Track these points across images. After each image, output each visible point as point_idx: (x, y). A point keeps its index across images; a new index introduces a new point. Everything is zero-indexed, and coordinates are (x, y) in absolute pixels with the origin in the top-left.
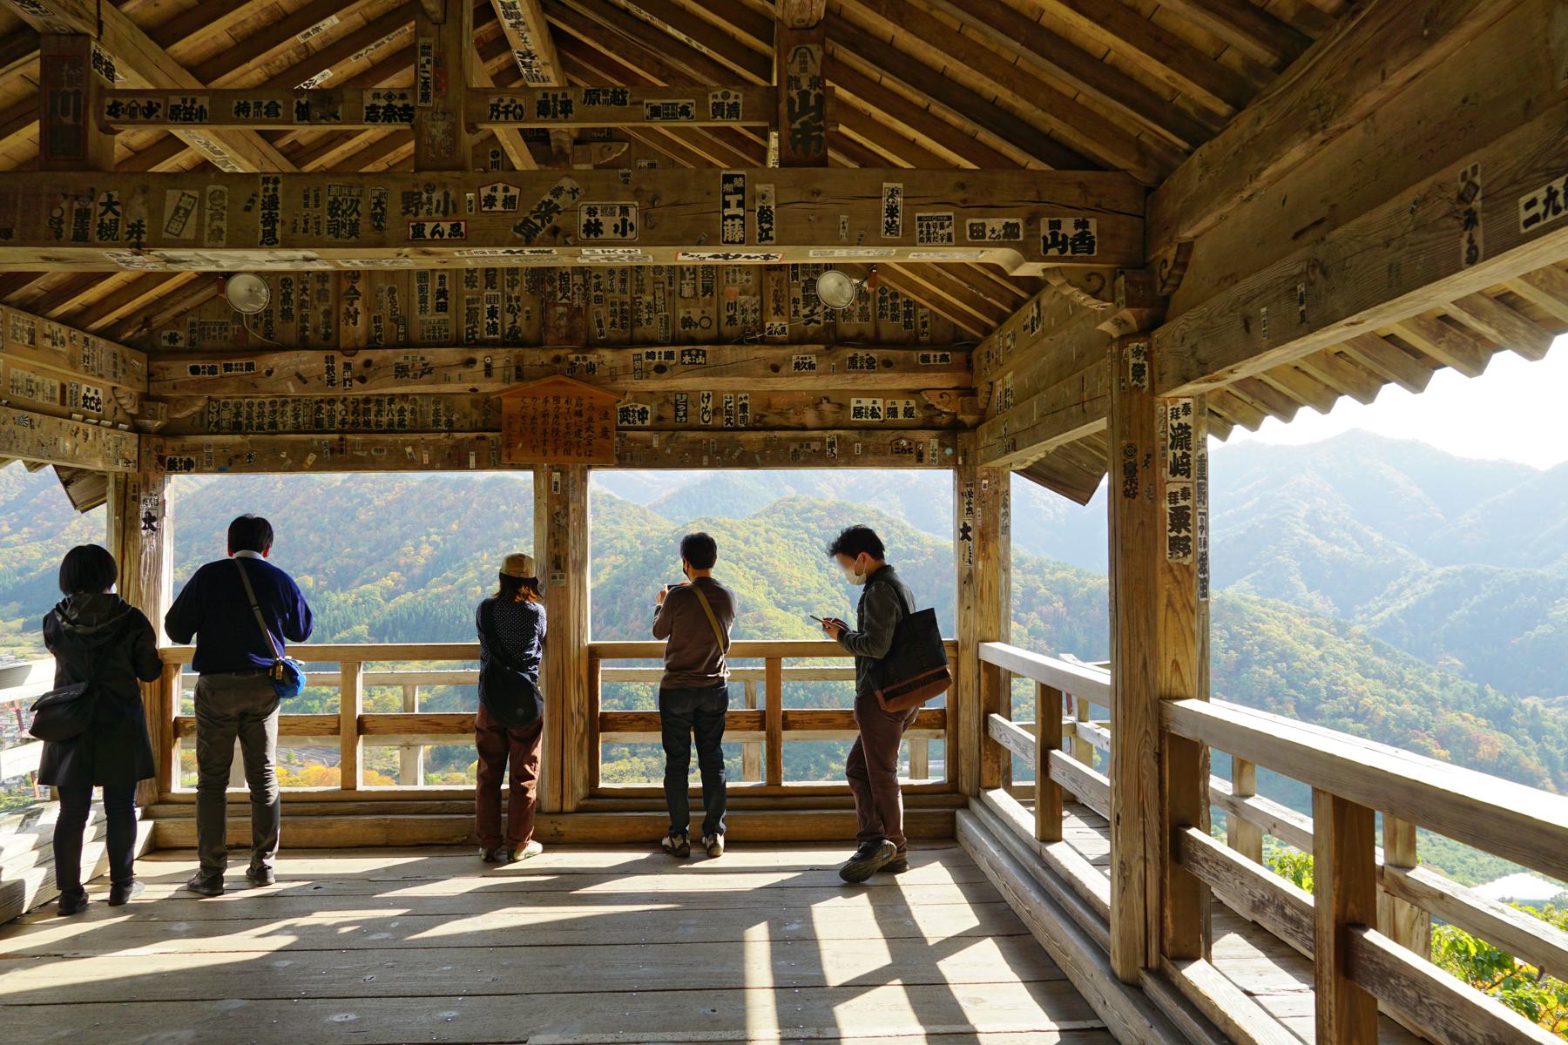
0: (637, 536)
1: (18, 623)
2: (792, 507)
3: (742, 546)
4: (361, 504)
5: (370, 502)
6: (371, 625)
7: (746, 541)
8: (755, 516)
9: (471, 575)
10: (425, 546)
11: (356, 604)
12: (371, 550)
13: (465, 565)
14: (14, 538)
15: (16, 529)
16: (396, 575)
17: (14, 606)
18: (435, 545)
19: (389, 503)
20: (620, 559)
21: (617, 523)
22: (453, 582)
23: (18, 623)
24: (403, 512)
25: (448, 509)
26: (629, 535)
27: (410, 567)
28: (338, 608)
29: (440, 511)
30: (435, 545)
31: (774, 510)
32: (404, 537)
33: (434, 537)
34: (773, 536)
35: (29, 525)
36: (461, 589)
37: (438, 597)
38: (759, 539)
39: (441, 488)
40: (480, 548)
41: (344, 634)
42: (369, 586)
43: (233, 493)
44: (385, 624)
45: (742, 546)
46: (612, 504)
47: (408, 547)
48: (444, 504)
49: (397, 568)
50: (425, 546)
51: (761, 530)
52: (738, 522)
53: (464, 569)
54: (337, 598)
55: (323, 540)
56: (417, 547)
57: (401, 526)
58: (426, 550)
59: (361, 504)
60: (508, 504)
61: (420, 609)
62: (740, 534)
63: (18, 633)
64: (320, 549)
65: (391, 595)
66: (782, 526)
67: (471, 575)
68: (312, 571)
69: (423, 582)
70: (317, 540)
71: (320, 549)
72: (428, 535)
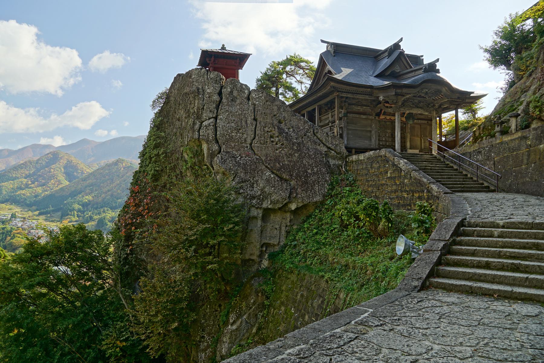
1: (37, 213)
14: (33, 185)
15: (33, 183)
17: (34, 208)
23: (37, 213)
35: (37, 181)
63: (37, 216)
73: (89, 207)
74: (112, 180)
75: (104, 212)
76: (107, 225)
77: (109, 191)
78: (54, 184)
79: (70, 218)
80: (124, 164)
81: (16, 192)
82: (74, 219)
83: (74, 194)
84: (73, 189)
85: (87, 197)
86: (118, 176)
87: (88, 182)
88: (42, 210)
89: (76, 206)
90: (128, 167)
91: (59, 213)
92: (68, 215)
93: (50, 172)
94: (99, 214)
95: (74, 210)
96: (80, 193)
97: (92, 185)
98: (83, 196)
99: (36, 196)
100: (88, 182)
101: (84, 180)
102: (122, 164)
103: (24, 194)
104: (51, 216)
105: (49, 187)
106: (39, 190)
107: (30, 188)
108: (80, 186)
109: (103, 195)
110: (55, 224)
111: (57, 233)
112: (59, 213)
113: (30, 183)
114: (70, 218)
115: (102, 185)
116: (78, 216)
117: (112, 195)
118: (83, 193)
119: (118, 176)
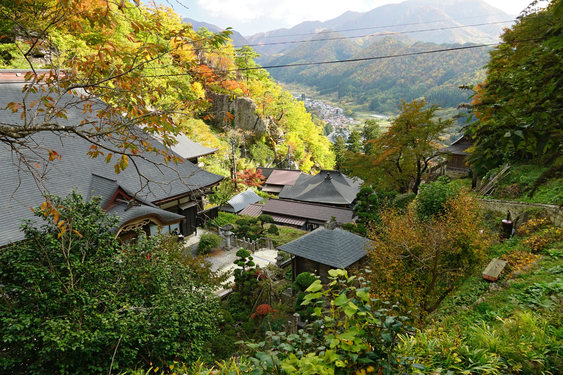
1: (319, 92)
11: (418, 89)
12: (422, 71)
16: (431, 80)
17: (315, 87)
18: (444, 69)
22: (453, 83)
23: (319, 92)
24: (433, 57)
25: (449, 55)
27: (436, 77)
29: (447, 56)
30: (444, 69)
37: (448, 88)
42: (423, 84)
43: (375, 51)
44: (430, 97)
49: (432, 77)
50: (441, 69)
55: (406, 67)
56: (438, 70)
57: (433, 62)
61: (442, 92)
64: (405, 70)
68: (403, 78)
69: (440, 83)
71: (405, 70)
73: (361, 87)
75: (375, 93)
77: (377, 71)
79: (346, 98)
80: (391, 42)
81: (299, 72)
84: (345, 69)
85: (359, 78)
89: (350, 87)
91: (337, 93)
92: (345, 95)
96: (352, 73)
98: (355, 77)
99: (315, 76)
103: (305, 74)
104: (330, 96)
111: (377, 133)
112: (337, 93)
115: (371, 65)
117: (381, 76)
118: (355, 74)
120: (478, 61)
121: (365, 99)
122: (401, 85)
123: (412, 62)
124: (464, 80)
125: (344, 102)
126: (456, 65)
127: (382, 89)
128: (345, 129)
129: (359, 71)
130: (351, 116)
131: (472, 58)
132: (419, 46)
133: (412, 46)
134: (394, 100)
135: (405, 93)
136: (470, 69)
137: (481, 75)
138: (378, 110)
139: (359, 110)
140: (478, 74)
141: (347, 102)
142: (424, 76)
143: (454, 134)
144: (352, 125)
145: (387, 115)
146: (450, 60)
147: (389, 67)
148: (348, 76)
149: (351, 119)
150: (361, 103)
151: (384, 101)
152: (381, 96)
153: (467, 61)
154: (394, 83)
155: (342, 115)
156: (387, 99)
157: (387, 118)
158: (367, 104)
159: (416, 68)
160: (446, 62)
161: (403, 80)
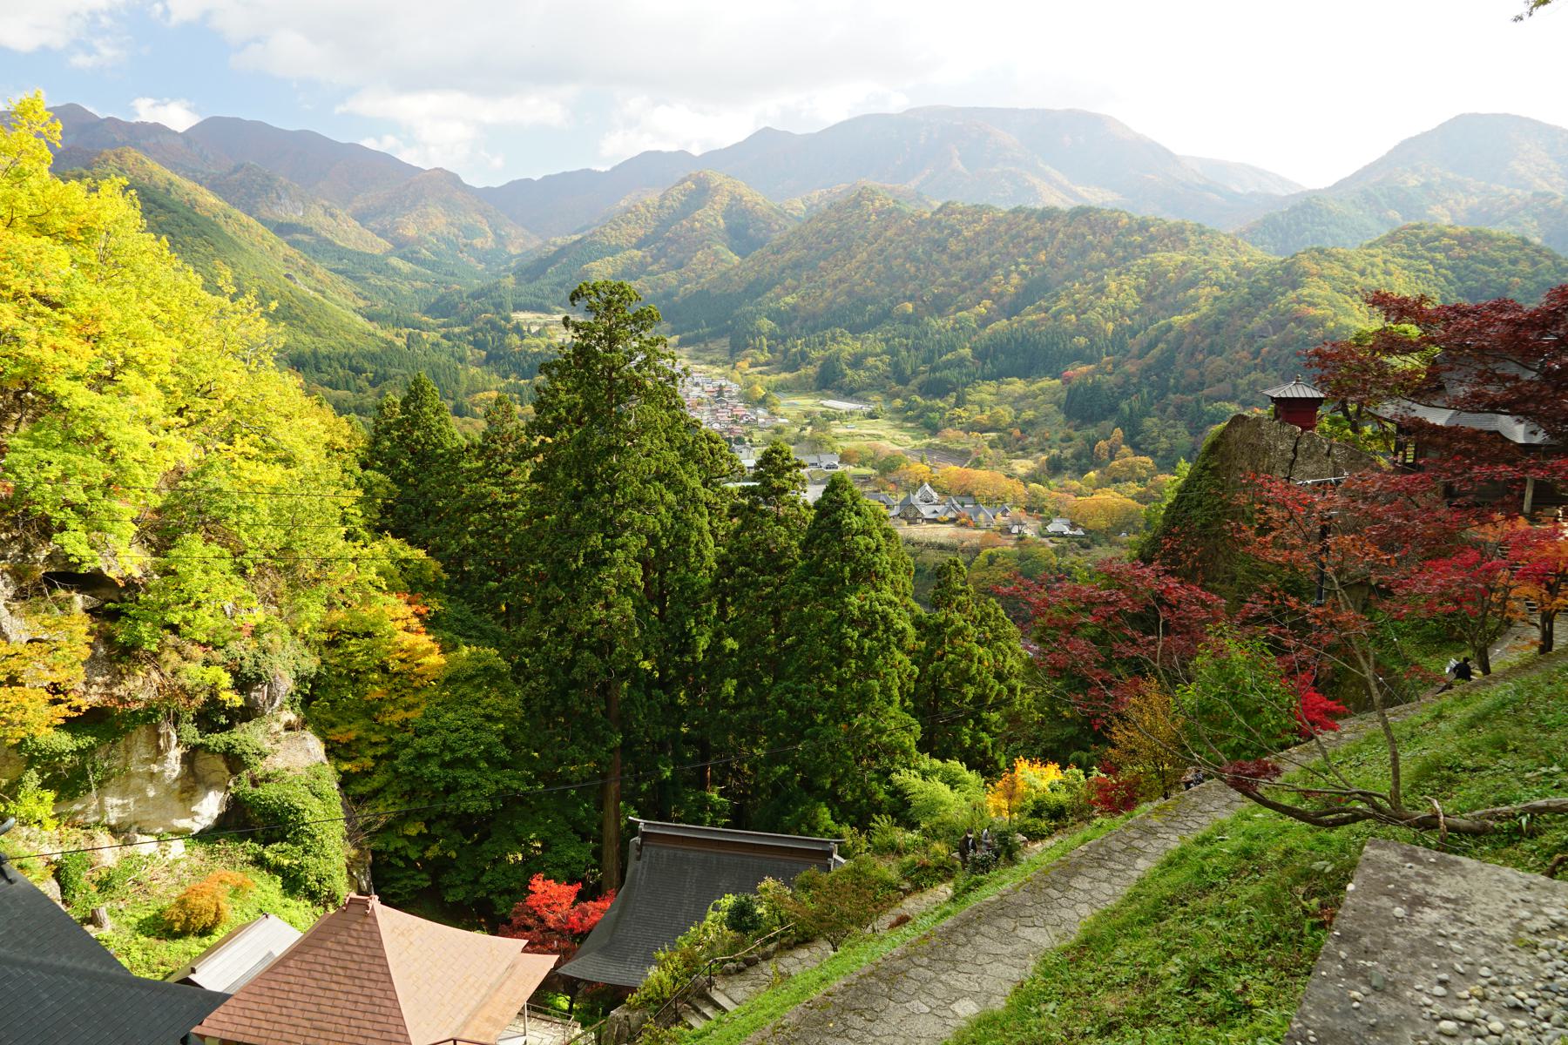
0: (1233, 268)
2: (1417, 236)
3: (1357, 277)
4: (951, 235)
5: (959, 232)
6: (973, 349)
7: (1362, 273)
8: (1370, 246)
9: (1063, 303)
10: (1014, 275)
11: (953, 329)
12: (963, 279)
13: (1057, 294)
14: (655, 267)
15: (656, 260)
16: (988, 302)
18: (1023, 274)
19: (977, 234)
20: (1216, 291)
21: (1206, 254)
24: (991, 244)
25: (1034, 239)
26: (1225, 265)
27: (1001, 295)
28: (938, 332)
29: (1027, 241)
30: (1023, 274)
31: (1392, 238)
32: (993, 267)
33: (1023, 267)
34: (1392, 267)
35: (665, 256)
36: (1055, 317)
37: (1034, 324)
38: (1376, 271)
39: (1026, 219)
40: (1070, 277)
41: (949, 356)
42: (965, 313)
43: (833, 226)
44: (987, 348)
45: (1357, 277)
46: (1203, 233)
47: (999, 276)
48: (1031, 234)
49: (989, 296)
50: (1014, 275)
51: (1378, 260)
52: (1353, 251)
53: (1057, 296)
54: (937, 323)
55: (918, 269)
57: (990, 256)
58: (1015, 279)
59: (951, 235)
60: (1094, 234)
61: (1019, 335)
62: (1356, 265)
65: (985, 322)
66: (1403, 256)
67: (1063, 303)
68: (910, 299)
69: (1013, 310)
70: (913, 269)
71: (913, 278)
72: (1017, 265)
73: (794, 325)
74: (848, 249)
75: (834, 339)
76: (845, 376)
77: (841, 281)
78: (704, 263)
80: (877, 204)
82: (762, 359)
83: (755, 289)
84: (752, 276)
85: (788, 299)
86: (863, 237)
87: (787, 256)
88: (686, 334)
89: (766, 324)
90: (890, 212)
91: (726, 341)
92: (747, 346)
93: (694, 230)
94: (822, 344)
95: (760, 333)
96: (769, 288)
97: (797, 265)
98: (778, 297)
99: (668, 295)
100: (787, 256)
101: (778, 251)
102: (872, 201)
104: (706, 350)
105: (693, 270)
106: (671, 278)
107: (650, 274)
108: (768, 269)
109: (828, 293)
110: (719, 371)
112: (726, 341)
113: (649, 260)
114: (752, 355)
115: (822, 263)
116: (771, 349)
117: (850, 293)
118: (778, 289)
119: (863, 237)
120: (1110, 254)
121: (804, 356)
122: (907, 319)
123: (935, 256)
124: (1076, 302)
125: (744, 365)
126: (1052, 263)
127: (856, 330)
128: (739, 441)
129: (789, 282)
130: (762, 402)
131: (1094, 248)
132: (953, 212)
133: (934, 214)
134: (886, 358)
135: (916, 338)
136: (1092, 275)
137: (1121, 290)
138: (840, 388)
139: (783, 388)
140: (1113, 286)
141: (752, 365)
142: (969, 293)
143: (1055, 451)
144: (761, 429)
145: (865, 400)
146: (1037, 250)
147: (870, 269)
148: (759, 295)
149: (760, 411)
150: (793, 367)
151: (857, 362)
152: (848, 346)
153: (1083, 253)
154: (885, 315)
155: (735, 401)
156: (865, 355)
157: (866, 409)
158: (810, 371)
159: (946, 273)
160: (1027, 256)
161: (909, 307)
